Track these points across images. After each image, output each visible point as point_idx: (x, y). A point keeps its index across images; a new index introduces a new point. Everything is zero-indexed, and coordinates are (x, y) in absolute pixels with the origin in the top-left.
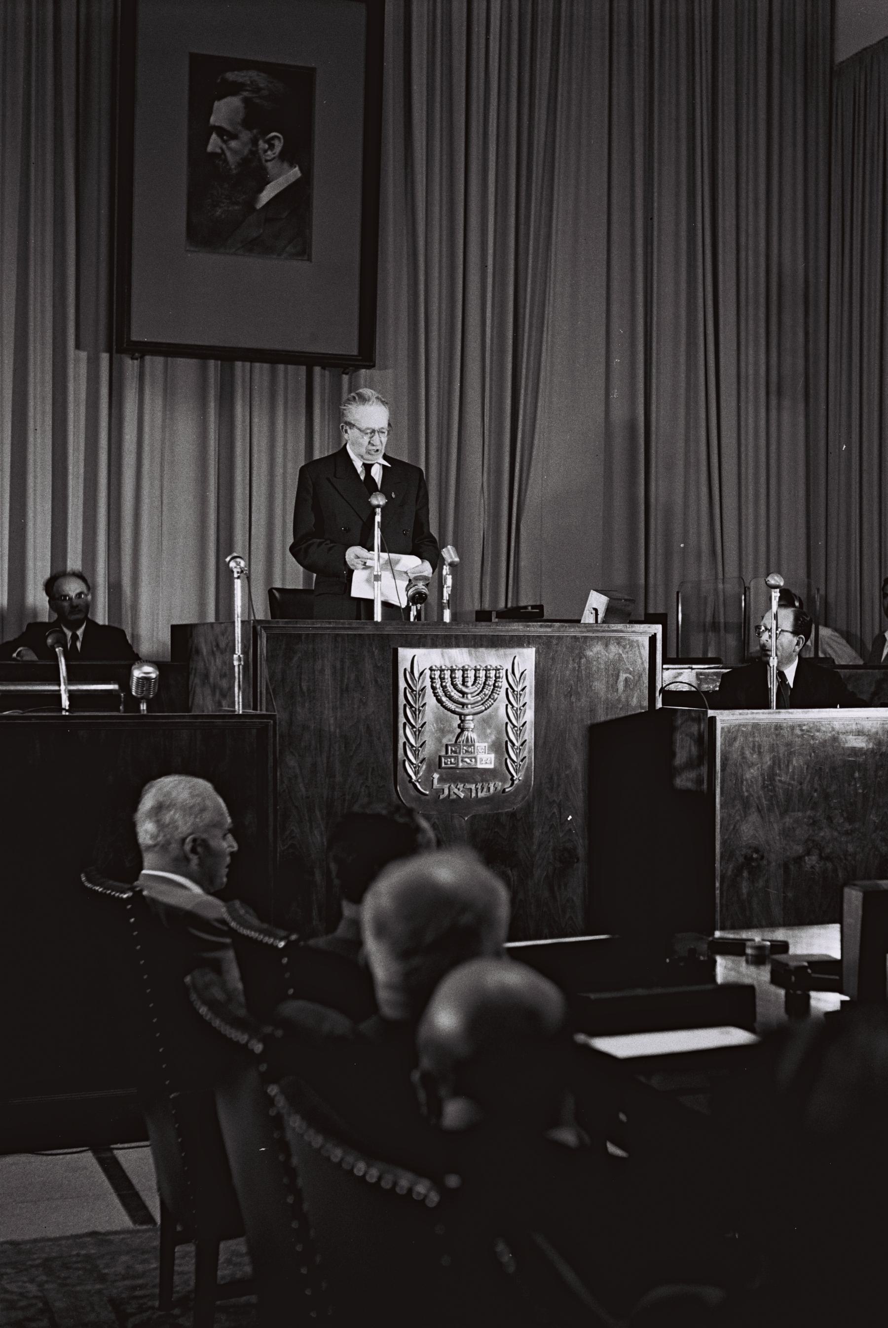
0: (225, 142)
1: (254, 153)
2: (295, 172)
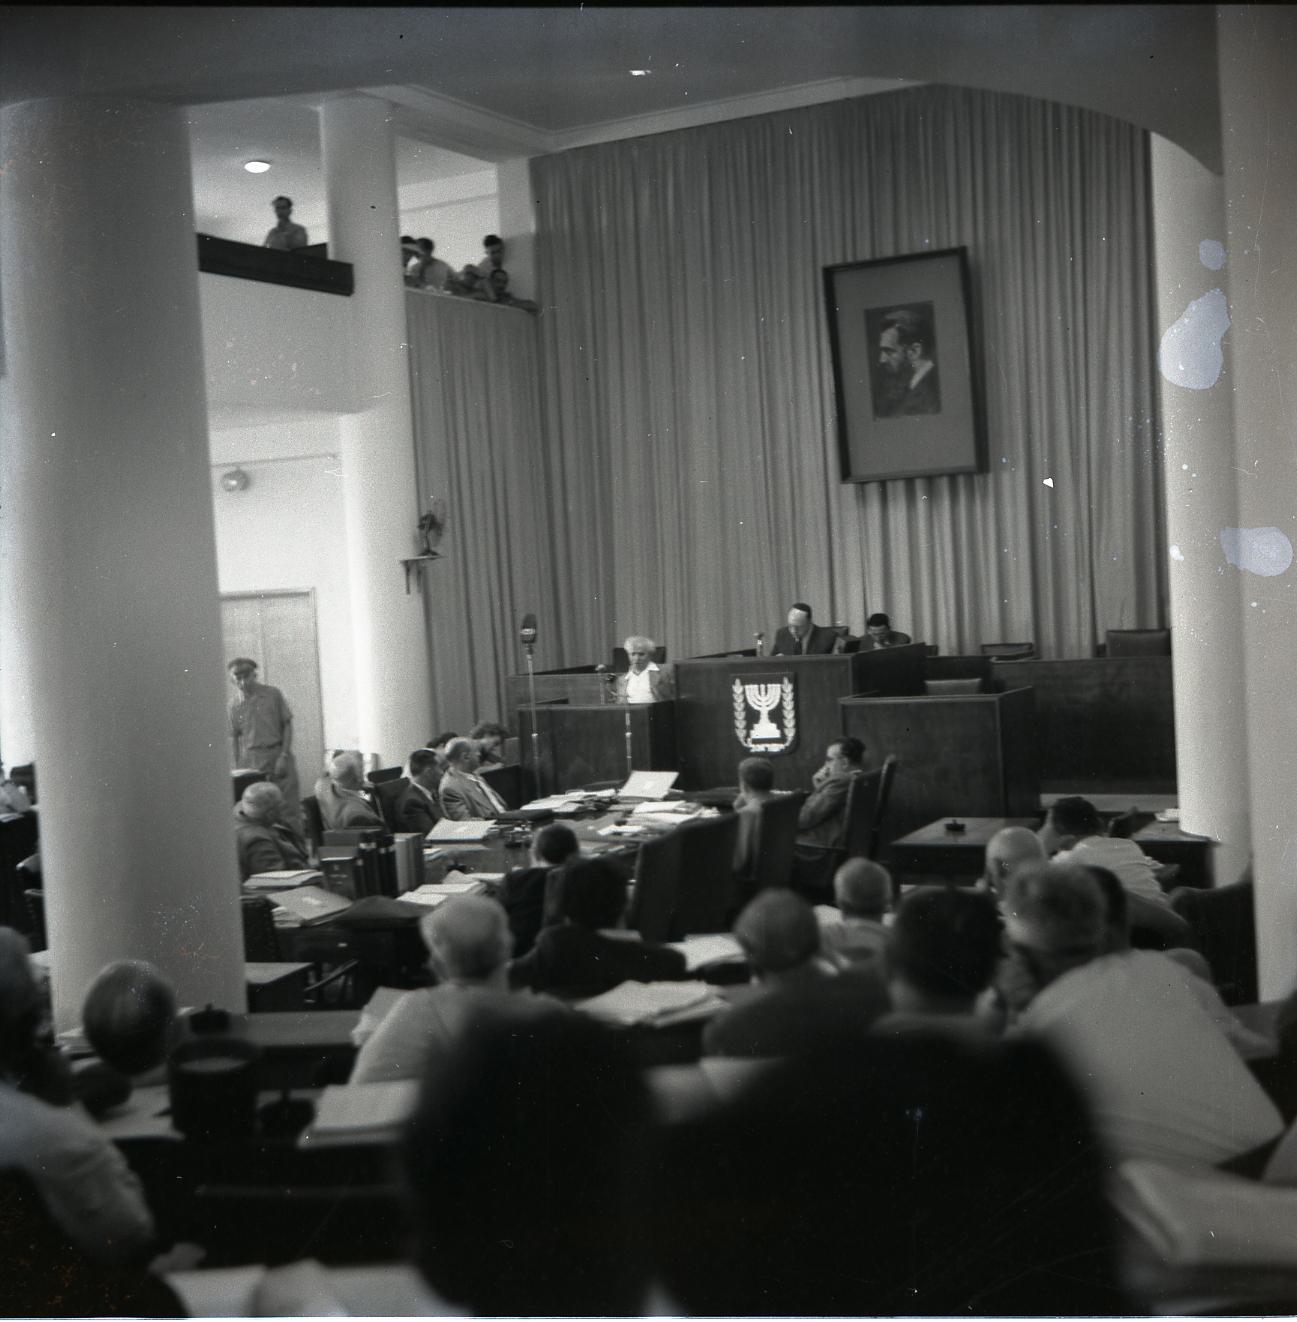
0: (889, 355)
1: (906, 358)
2: (928, 365)
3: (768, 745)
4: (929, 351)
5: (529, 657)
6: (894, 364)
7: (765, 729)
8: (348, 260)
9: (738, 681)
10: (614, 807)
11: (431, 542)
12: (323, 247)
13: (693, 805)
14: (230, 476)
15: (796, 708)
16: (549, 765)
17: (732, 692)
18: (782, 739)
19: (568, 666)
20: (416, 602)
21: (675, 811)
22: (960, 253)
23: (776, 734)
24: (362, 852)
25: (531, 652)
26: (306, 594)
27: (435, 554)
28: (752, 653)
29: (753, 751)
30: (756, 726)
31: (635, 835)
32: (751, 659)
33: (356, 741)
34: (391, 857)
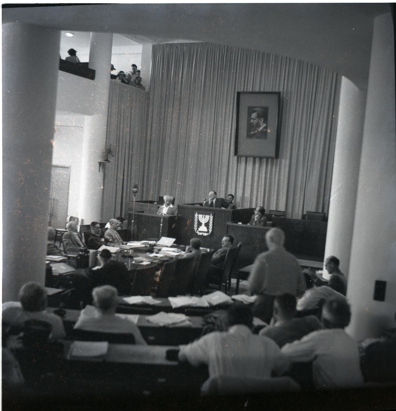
0: (254, 121)
1: (258, 122)
2: (265, 125)
3: (203, 233)
4: (266, 121)
5: (134, 197)
6: (255, 123)
7: (203, 228)
9: (197, 213)
10: (155, 247)
11: (108, 157)
12: (86, 64)
13: (179, 250)
15: (213, 223)
16: (136, 230)
17: (194, 216)
18: (208, 232)
19: (144, 200)
20: (101, 174)
21: (174, 251)
22: (279, 94)
23: (206, 230)
24: (80, 255)
25: (135, 196)
26: (68, 168)
27: (109, 161)
28: (201, 204)
29: (198, 234)
30: (200, 227)
31: (161, 257)
32: (201, 207)
33: (77, 214)
34: (88, 257)
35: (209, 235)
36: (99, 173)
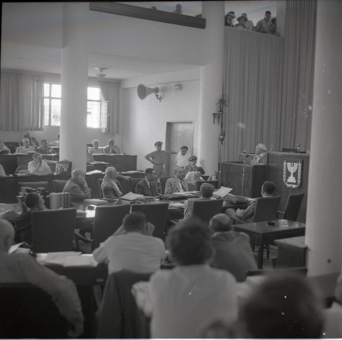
3: (292, 185)
7: (292, 179)
8: (205, 18)
9: (285, 161)
12: (201, 15)
14: (176, 85)
18: (296, 184)
23: (294, 181)
26: (191, 123)
29: (287, 186)
30: (289, 177)
35: (298, 186)
36: (214, 125)
